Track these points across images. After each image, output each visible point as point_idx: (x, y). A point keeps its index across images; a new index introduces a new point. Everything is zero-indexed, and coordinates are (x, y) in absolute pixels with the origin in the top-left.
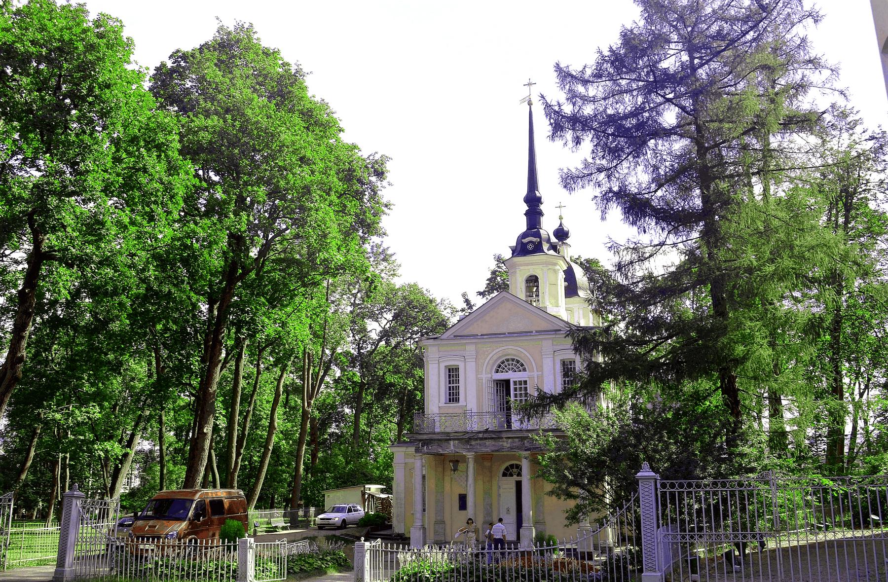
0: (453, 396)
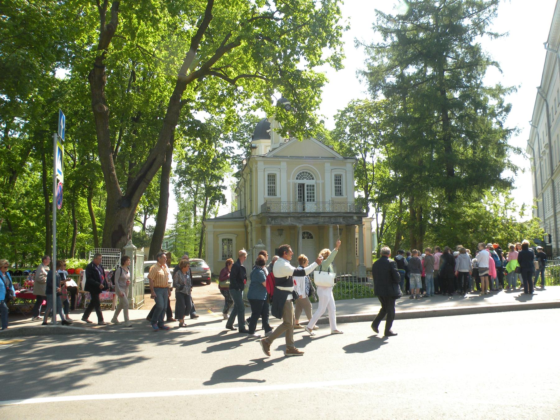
0: (272, 191)
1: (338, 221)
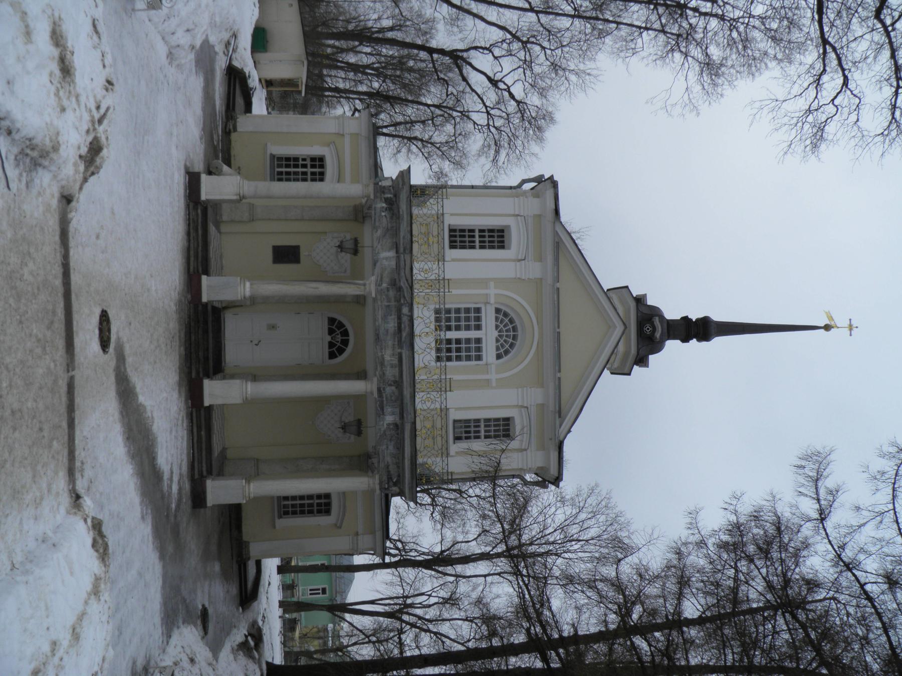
0: (462, 238)
1: (388, 410)
